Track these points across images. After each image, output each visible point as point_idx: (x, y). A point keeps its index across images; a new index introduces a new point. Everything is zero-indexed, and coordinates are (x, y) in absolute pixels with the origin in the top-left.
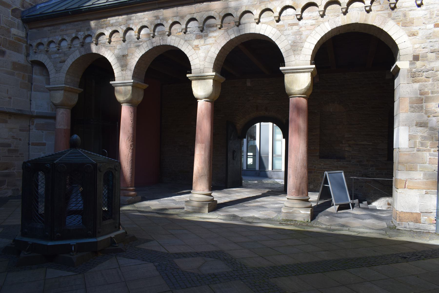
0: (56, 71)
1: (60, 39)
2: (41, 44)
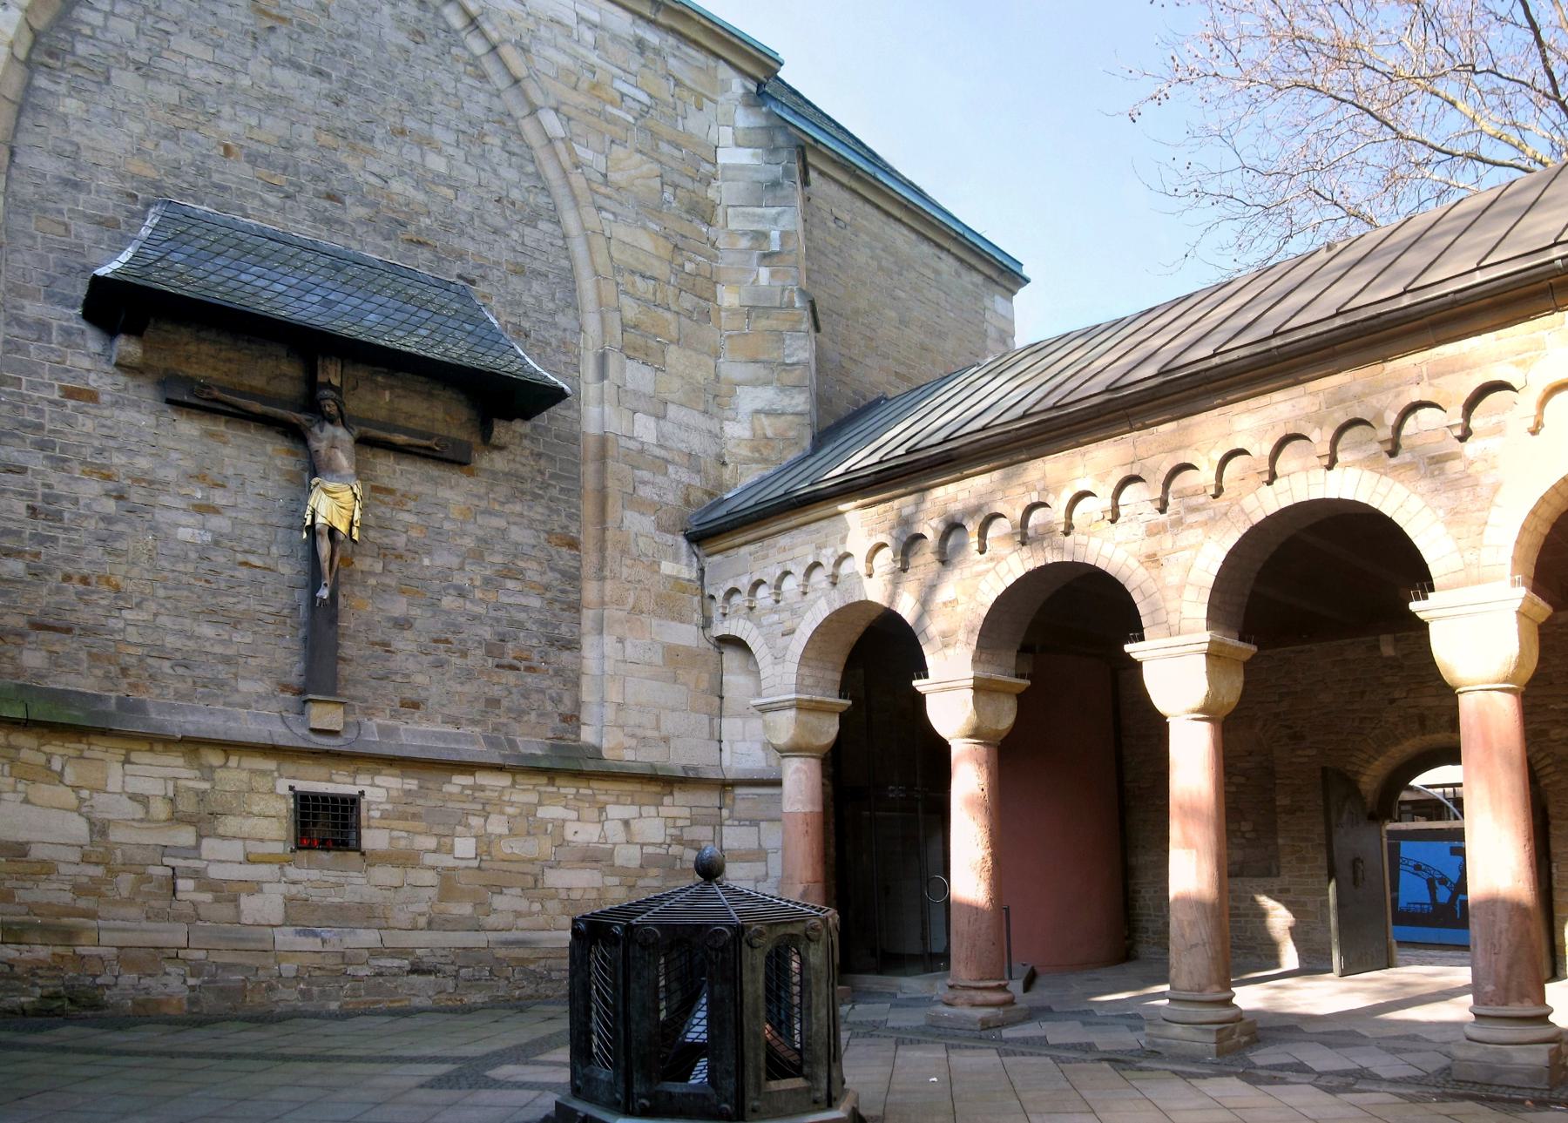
2: (734, 591)
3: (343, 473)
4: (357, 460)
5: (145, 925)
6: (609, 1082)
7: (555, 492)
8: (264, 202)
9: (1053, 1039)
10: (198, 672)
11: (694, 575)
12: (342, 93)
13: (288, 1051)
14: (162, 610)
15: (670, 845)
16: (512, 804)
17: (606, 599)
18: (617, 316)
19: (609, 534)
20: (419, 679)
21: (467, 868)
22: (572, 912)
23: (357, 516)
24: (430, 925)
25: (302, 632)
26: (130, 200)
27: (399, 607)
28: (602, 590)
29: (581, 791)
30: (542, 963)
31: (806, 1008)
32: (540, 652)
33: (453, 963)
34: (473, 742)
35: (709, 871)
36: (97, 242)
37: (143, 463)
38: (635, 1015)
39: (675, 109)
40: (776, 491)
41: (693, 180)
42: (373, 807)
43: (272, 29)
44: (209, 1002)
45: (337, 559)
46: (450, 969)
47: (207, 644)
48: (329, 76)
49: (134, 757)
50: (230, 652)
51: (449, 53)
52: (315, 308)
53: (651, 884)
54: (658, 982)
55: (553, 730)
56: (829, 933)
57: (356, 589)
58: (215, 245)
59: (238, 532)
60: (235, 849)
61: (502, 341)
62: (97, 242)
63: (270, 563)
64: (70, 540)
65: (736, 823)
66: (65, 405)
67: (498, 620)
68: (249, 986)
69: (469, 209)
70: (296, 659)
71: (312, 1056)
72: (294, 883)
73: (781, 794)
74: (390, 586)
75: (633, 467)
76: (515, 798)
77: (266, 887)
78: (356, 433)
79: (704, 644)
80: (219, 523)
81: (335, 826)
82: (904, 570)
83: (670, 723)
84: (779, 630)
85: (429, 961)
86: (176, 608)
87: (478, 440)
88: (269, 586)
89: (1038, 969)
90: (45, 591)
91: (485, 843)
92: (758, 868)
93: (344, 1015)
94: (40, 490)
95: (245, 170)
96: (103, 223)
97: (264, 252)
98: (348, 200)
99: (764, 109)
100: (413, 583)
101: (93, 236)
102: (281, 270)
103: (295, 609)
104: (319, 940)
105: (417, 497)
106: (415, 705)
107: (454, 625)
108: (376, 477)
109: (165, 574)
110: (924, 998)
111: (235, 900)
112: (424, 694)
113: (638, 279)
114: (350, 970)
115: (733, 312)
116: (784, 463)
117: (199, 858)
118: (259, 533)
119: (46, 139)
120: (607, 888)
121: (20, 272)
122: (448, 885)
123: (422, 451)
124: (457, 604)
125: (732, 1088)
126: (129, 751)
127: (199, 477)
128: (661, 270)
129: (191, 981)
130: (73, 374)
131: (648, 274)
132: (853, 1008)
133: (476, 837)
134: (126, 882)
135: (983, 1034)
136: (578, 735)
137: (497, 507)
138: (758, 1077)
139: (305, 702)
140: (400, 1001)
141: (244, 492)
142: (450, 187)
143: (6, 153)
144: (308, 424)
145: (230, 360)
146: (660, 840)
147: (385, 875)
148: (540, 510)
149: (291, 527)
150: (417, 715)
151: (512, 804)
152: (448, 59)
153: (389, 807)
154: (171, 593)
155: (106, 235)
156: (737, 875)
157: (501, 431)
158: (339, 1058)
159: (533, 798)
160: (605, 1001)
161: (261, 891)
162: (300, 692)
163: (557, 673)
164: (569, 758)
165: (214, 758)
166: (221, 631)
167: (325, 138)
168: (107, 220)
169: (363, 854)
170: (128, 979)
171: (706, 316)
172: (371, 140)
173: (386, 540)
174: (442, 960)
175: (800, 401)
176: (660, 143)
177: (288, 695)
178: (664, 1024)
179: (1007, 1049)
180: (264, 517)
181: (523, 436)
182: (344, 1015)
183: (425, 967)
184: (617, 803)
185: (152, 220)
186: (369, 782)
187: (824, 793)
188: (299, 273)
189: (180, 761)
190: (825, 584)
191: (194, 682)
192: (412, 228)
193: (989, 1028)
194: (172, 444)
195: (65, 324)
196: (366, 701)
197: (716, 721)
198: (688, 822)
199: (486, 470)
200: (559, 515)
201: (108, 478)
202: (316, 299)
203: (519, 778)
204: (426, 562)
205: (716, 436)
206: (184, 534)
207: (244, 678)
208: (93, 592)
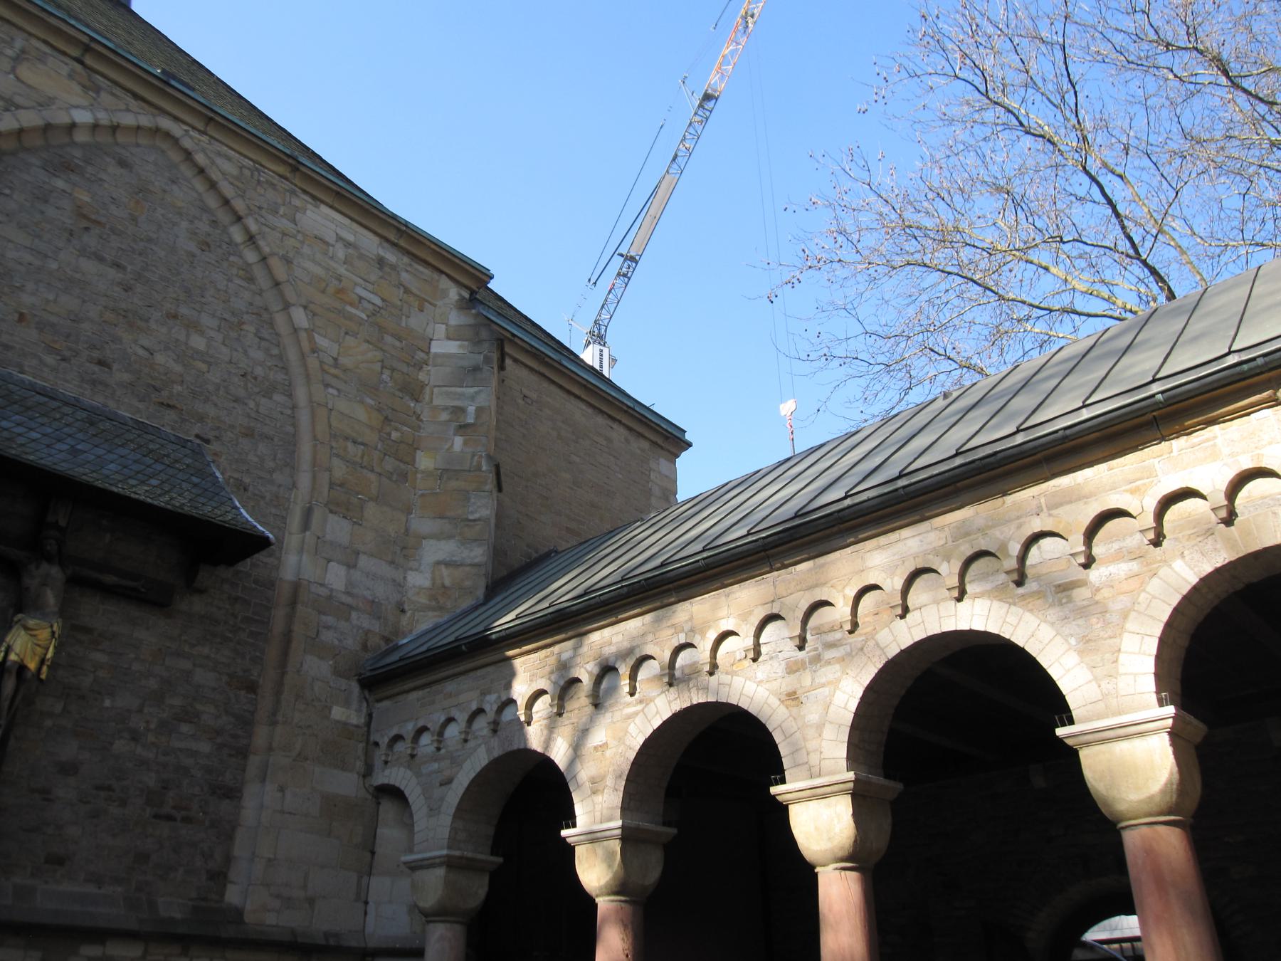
0: (431, 810)
1: (443, 719)
8: (41, 361)
11: (362, 720)
12: (132, 282)
23: (50, 655)
39: (401, 310)
41: (408, 364)
43: (87, 229)
45: (19, 698)
48: (124, 268)
51: (227, 260)
69: (218, 381)
75: (320, 613)
82: (560, 714)
98: (115, 367)
99: (473, 311)
102: (40, 420)
113: (350, 445)
115: (428, 474)
116: (458, 611)
131: (360, 440)
136: (222, 895)
137: (187, 649)
142: (204, 362)
152: (225, 264)
167: (109, 316)
171: (404, 477)
172: (147, 321)
175: (478, 554)
176: (385, 335)
190: (486, 732)
192: (165, 393)
197: (365, 879)
202: (65, 447)
204: (107, 703)
205: (400, 585)
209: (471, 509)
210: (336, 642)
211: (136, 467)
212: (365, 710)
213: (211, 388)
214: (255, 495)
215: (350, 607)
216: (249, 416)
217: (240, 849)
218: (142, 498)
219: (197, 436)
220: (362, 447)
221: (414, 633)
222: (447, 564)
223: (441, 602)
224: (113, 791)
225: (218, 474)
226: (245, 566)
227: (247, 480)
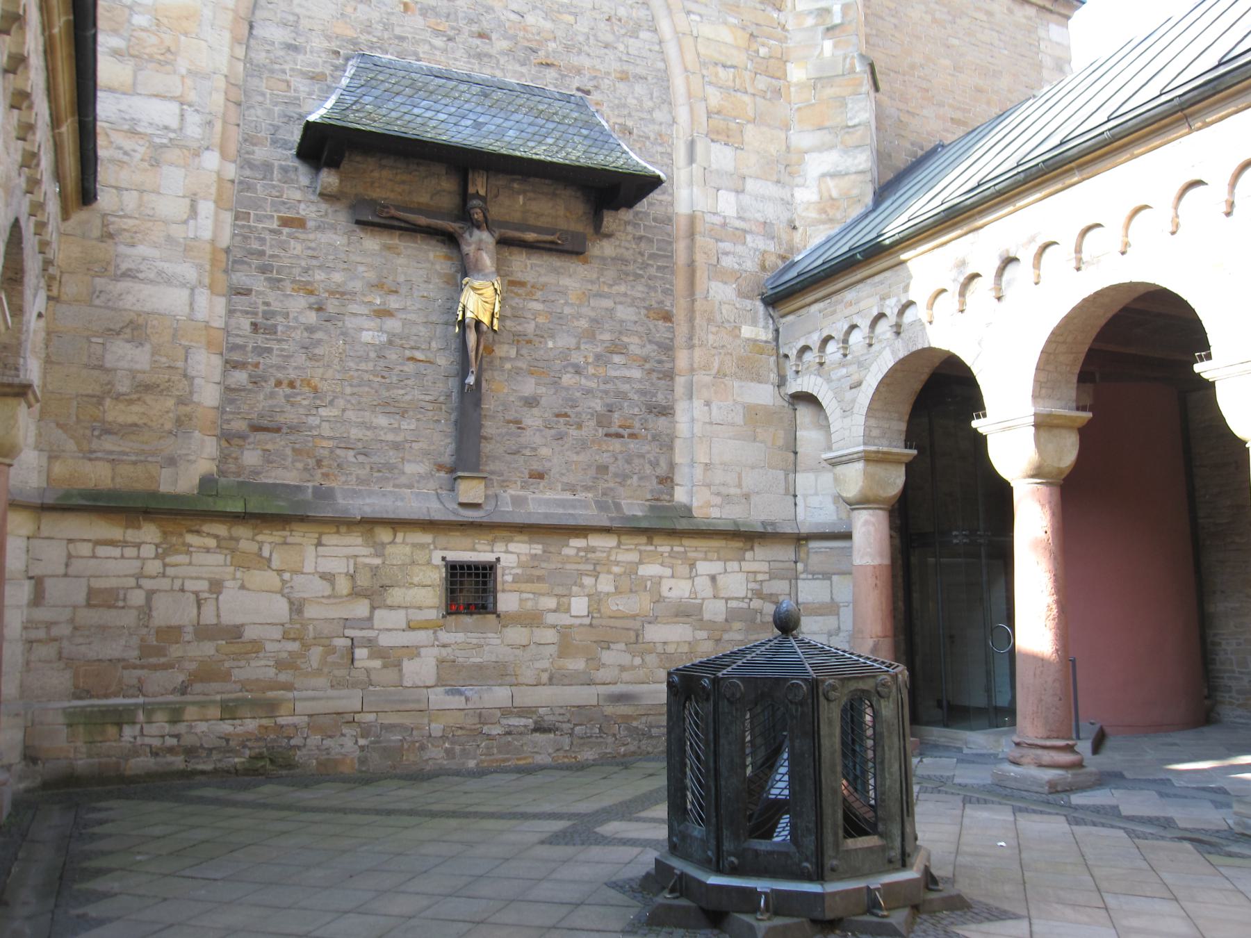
1: (846, 327)
3: (487, 271)
4: (498, 259)
5: (330, 692)
6: (702, 840)
7: (652, 271)
8: (433, 47)
9: (1126, 810)
10: (375, 459)
13: (436, 807)
14: (349, 406)
15: (751, 600)
16: (617, 563)
17: (695, 366)
18: (703, 105)
19: (698, 304)
20: (544, 451)
21: (581, 625)
22: (667, 665)
23: (497, 309)
24: (551, 681)
25: (453, 417)
26: (334, 56)
27: (528, 387)
28: (692, 358)
29: (676, 549)
30: (644, 719)
31: (880, 762)
32: (640, 420)
33: (569, 721)
34: (587, 507)
35: (786, 624)
36: (310, 94)
37: (337, 277)
38: (724, 770)
40: (841, 248)
42: (507, 572)
44: (376, 762)
45: (481, 347)
46: (566, 726)
47: (382, 433)
49: (325, 539)
50: (399, 438)
52: (468, 131)
53: (736, 638)
54: (744, 738)
55: (652, 491)
56: (899, 690)
57: (496, 374)
58: (396, 86)
59: (406, 331)
60: (398, 619)
61: (611, 141)
62: (310, 94)
63: (431, 356)
64: (282, 350)
65: (810, 576)
66: (281, 233)
67: (606, 392)
68: (406, 746)
69: (586, 30)
70: (449, 440)
71: (454, 812)
72: (444, 646)
73: (851, 548)
74: (521, 369)
75: (717, 240)
76: (621, 557)
77: (423, 651)
78: (497, 235)
79: (780, 402)
80: (393, 324)
81: (477, 591)
83: (751, 480)
84: (847, 383)
85: (550, 719)
86: (359, 403)
87: (592, 231)
88: (429, 377)
89: (1107, 730)
90: (261, 397)
91: (596, 599)
92: (831, 622)
93: (480, 773)
94: (262, 308)
95: (419, 21)
96: (315, 78)
97: (431, 88)
98: (494, 36)
100: (540, 364)
101: (307, 89)
102: (443, 101)
103: (449, 396)
104: (463, 698)
105: (544, 286)
106: (540, 476)
107: (572, 400)
108: (512, 273)
109: (352, 373)
110: (990, 755)
111: (398, 665)
112: (548, 465)
113: (720, 70)
114: (486, 729)
115: (801, 86)
116: (849, 221)
117: (372, 628)
118: (423, 331)
119: (276, 13)
120: (697, 641)
121: (253, 125)
122: (565, 647)
123: (548, 246)
124: (574, 381)
125: (812, 847)
126: (321, 534)
127: (378, 286)
128: (739, 58)
129: (362, 742)
130: (287, 206)
131: (729, 63)
132: (921, 761)
133: (588, 596)
134: (316, 653)
135: (1051, 797)
136: (672, 496)
137: (606, 289)
138: (836, 834)
139: (455, 479)
140: (525, 758)
141: (412, 295)
142: (571, 13)
143: (247, 27)
144: (460, 231)
145: (403, 182)
146: (742, 594)
147: (516, 634)
148: (640, 288)
149: (446, 323)
150: (543, 483)
151: (617, 563)
153: (519, 571)
154: (355, 390)
155: (316, 88)
156: (812, 629)
157: (610, 220)
158: (476, 815)
159: (633, 557)
160: (698, 758)
161: (418, 655)
162: (452, 470)
163: (654, 438)
164: (665, 517)
165: (384, 535)
166: (393, 421)
168: (318, 74)
169: (498, 616)
170: (315, 739)
171: (778, 92)
173: (519, 328)
174: (560, 718)
175: (863, 160)
177: (442, 474)
178: (750, 780)
179: (1076, 816)
180: (426, 316)
181: (627, 223)
182: (480, 773)
183: (545, 725)
184: (705, 559)
185: (350, 71)
186: (503, 549)
187: (892, 546)
188: (457, 103)
189: (359, 540)
190: (889, 334)
191: (371, 468)
192: (542, 53)
193: (1057, 792)
194: (359, 259)
195: (283, 163)
196: (502, 475)
197: (791, 476)
198: (767, 577)
199: (597, 257)
200: (656, 291)
201: (311, 293)
202: (469, 123)
203: (624, 539)
204: (550, 344)
205: (788, 203)
206: (367, 337)
207: (409, 461)
208: (298, 394)
209: (849, 115)
210: (736, 267)
211: (531, 130)
212: (771, 326)
213: (581, 39)
214: (640, 136)
215: (745, 231)
216: (621, 60)
217: (680, 457)
218: (542, 157)
219: (578, 89)
220: (732, 70)
221: (808, 248)
222: (833, 175)
223: (831, 214)
224: (569, 416)
225: (604, 123)
226: (643, 206)
227: (630, 123)
